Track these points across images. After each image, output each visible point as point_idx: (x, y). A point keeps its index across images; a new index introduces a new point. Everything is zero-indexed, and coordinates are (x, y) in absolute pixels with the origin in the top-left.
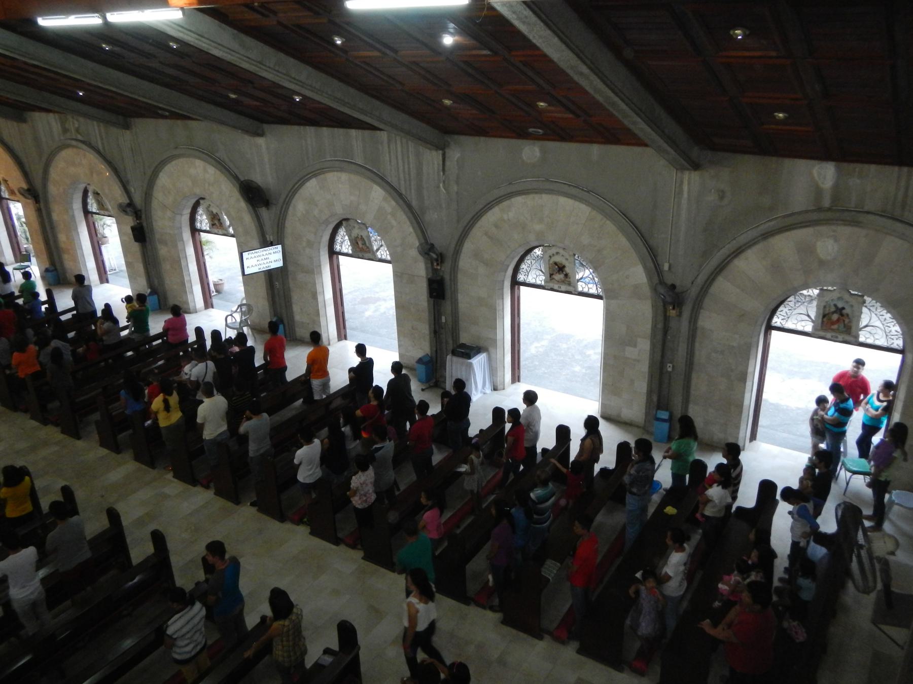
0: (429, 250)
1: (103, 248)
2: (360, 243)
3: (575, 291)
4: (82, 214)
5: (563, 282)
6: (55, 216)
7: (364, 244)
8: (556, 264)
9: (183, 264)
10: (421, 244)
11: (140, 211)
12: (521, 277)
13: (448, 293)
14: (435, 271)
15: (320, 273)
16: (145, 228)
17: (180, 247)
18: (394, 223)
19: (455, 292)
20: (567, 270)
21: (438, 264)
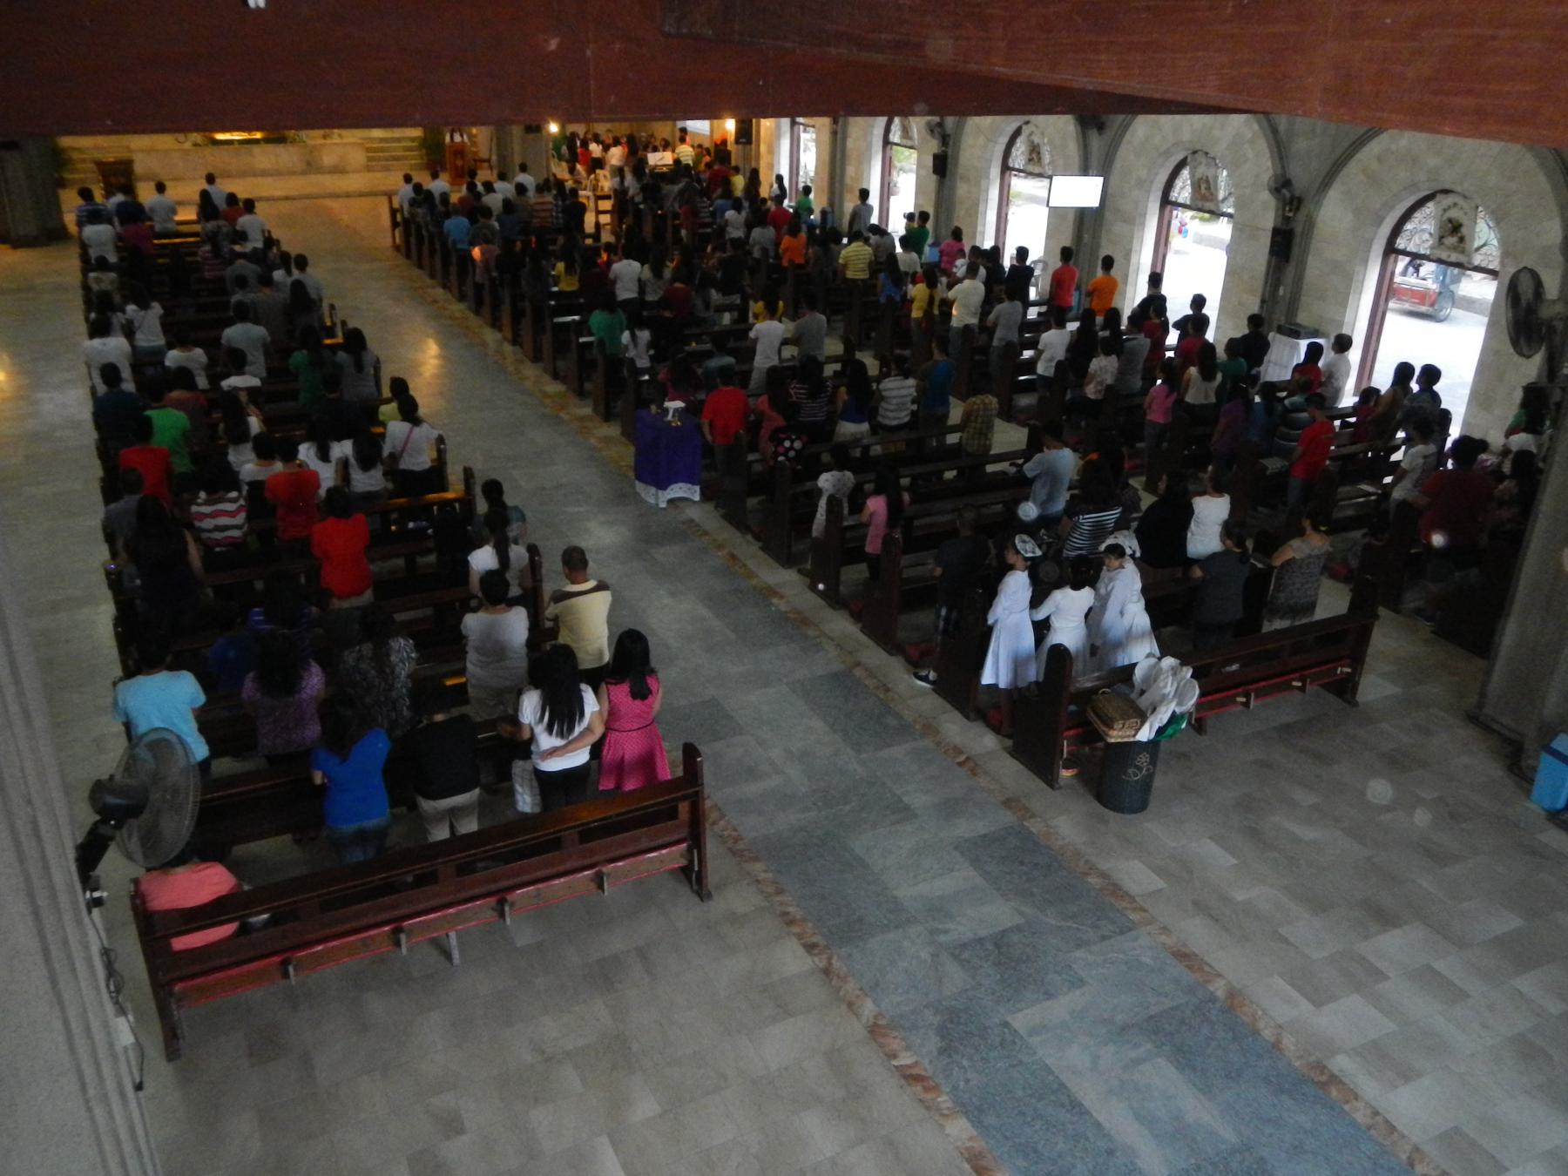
0: (1282, 187)
1: (892, 199)
2: (1203, 186)
3: (1470, 263)
4: (881, 143)
5: (1454, 248)
6: (850, 143)
7: (1208, 188)
8: (1450, 221)
9: (981, 208)
10: (1276, 176)
11: (949, 136)
12: (1401, 243)
13: (1295, 251)
14: (1287, 220)
15: (1143, 225)
16: (949, 160)
17: (983, 183)
18: (1250, 155)
19: (1305, 251)
20: (1464, 230)
21: (1290, 210)
